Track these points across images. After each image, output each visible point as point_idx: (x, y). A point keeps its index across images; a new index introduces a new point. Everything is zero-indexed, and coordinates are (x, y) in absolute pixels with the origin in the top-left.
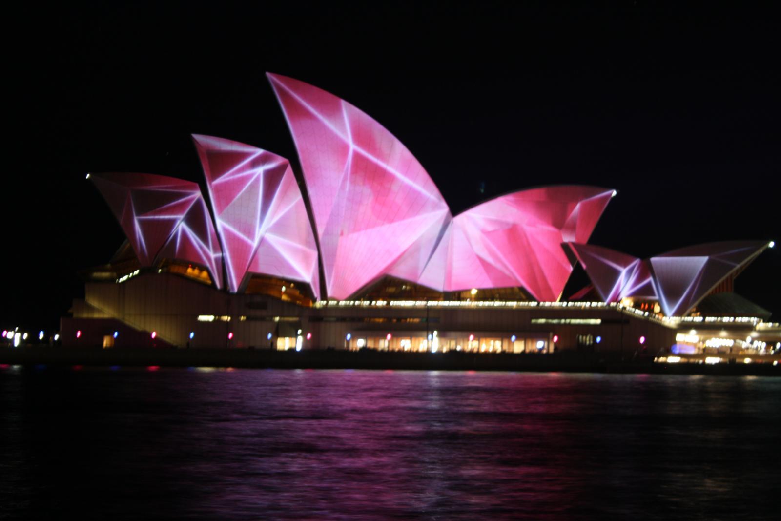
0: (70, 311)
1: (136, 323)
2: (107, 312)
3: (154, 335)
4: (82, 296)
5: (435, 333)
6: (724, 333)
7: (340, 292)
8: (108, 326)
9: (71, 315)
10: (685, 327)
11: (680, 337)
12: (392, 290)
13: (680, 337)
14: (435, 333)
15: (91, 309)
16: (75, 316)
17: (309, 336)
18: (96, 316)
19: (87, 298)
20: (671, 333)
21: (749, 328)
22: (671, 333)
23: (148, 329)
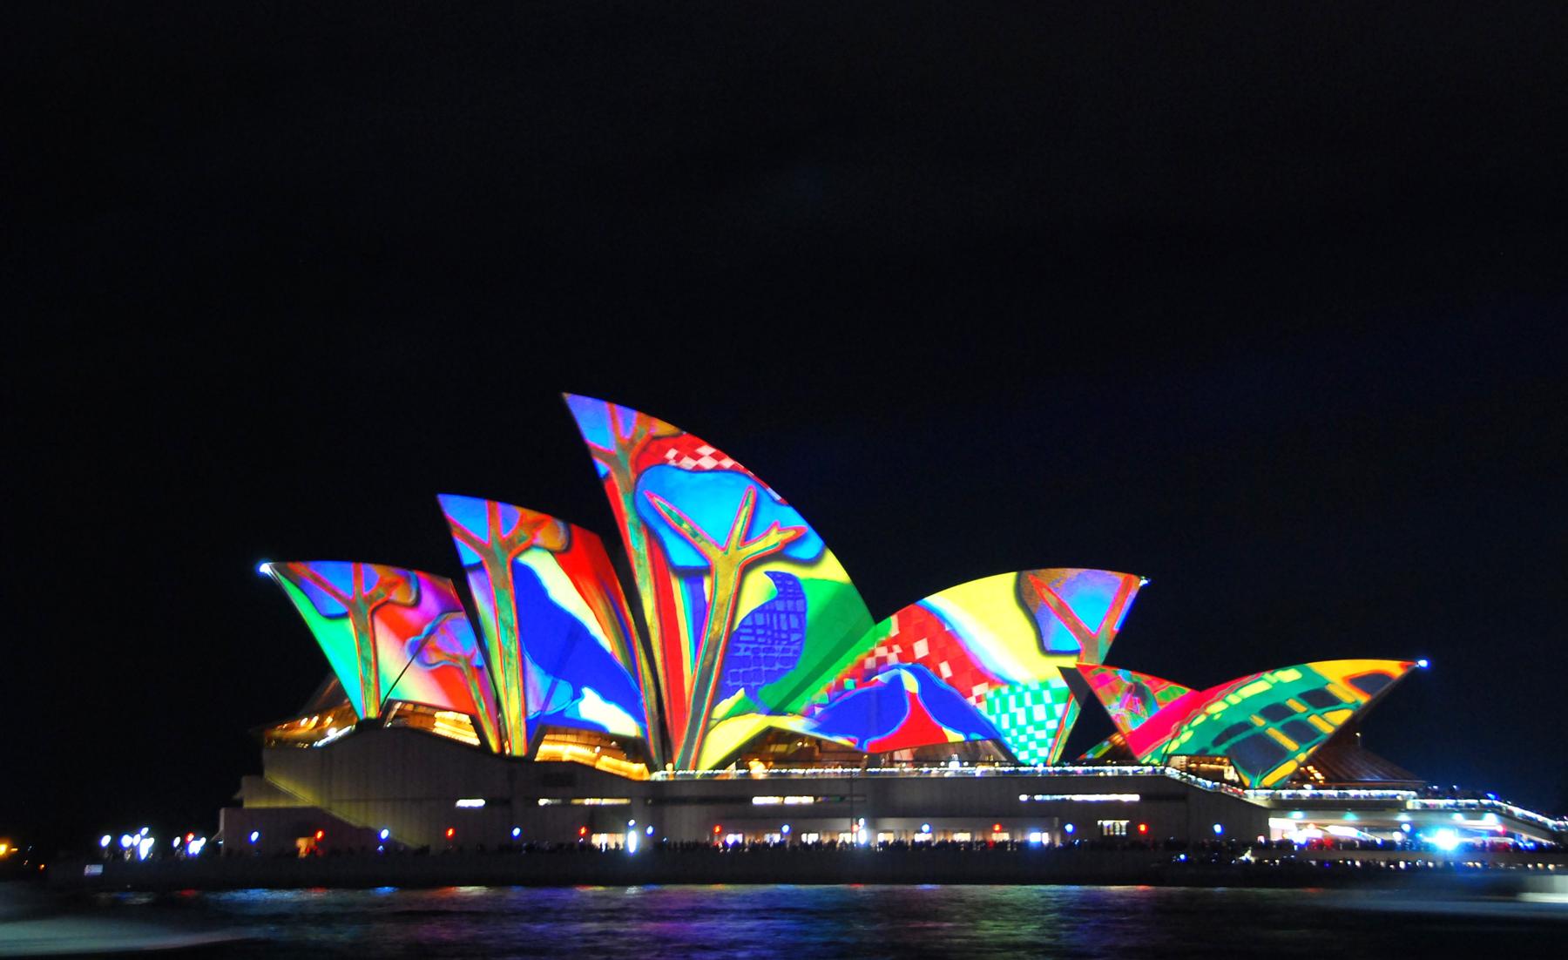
0: (237, 796)
1: (351, 814)
2: (304, 797)
3: (385, 834)
4: (257, 770)
5: (862, 821)
6: (1351, 817)
8: (304, 821)
9: (240, 803)
12: (781, 748)
14: (862, 821)
15: (274, 792)
16: (246, 805)
17: (650, 830)
18: (282, 804)
19: (266, 773)
20: (1259, 816)
21: (1399, 806)
22: (1259, 816)
23: (372, 825)
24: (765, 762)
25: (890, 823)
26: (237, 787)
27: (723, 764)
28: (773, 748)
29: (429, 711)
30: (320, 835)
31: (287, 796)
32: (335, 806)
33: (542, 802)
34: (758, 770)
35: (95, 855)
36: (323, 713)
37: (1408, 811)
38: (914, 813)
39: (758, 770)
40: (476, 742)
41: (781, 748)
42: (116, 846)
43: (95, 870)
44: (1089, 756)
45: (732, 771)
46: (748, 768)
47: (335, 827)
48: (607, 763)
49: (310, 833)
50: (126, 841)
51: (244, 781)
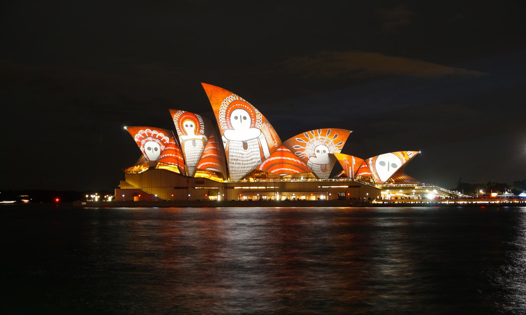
2: (135, 186)
4: (124, 179)
6: (401, 191)
8: (136, 192)
10: (385, 189)
12: (257, 174)
15: (128, 185)
18: (130, 188)
24: (253, 178)
25: (285, 193)
26: (119, 184)
27: (243, 179)
32: (144, 188)
34: (252, 180)
35: (85, 199)
39: (252, 180)
41: (257, 174)
42: (90, 198)
43: (85, 203)
47: (144, 194)
48: (213, 178)
49: (137, 195)
50: (92, 196)
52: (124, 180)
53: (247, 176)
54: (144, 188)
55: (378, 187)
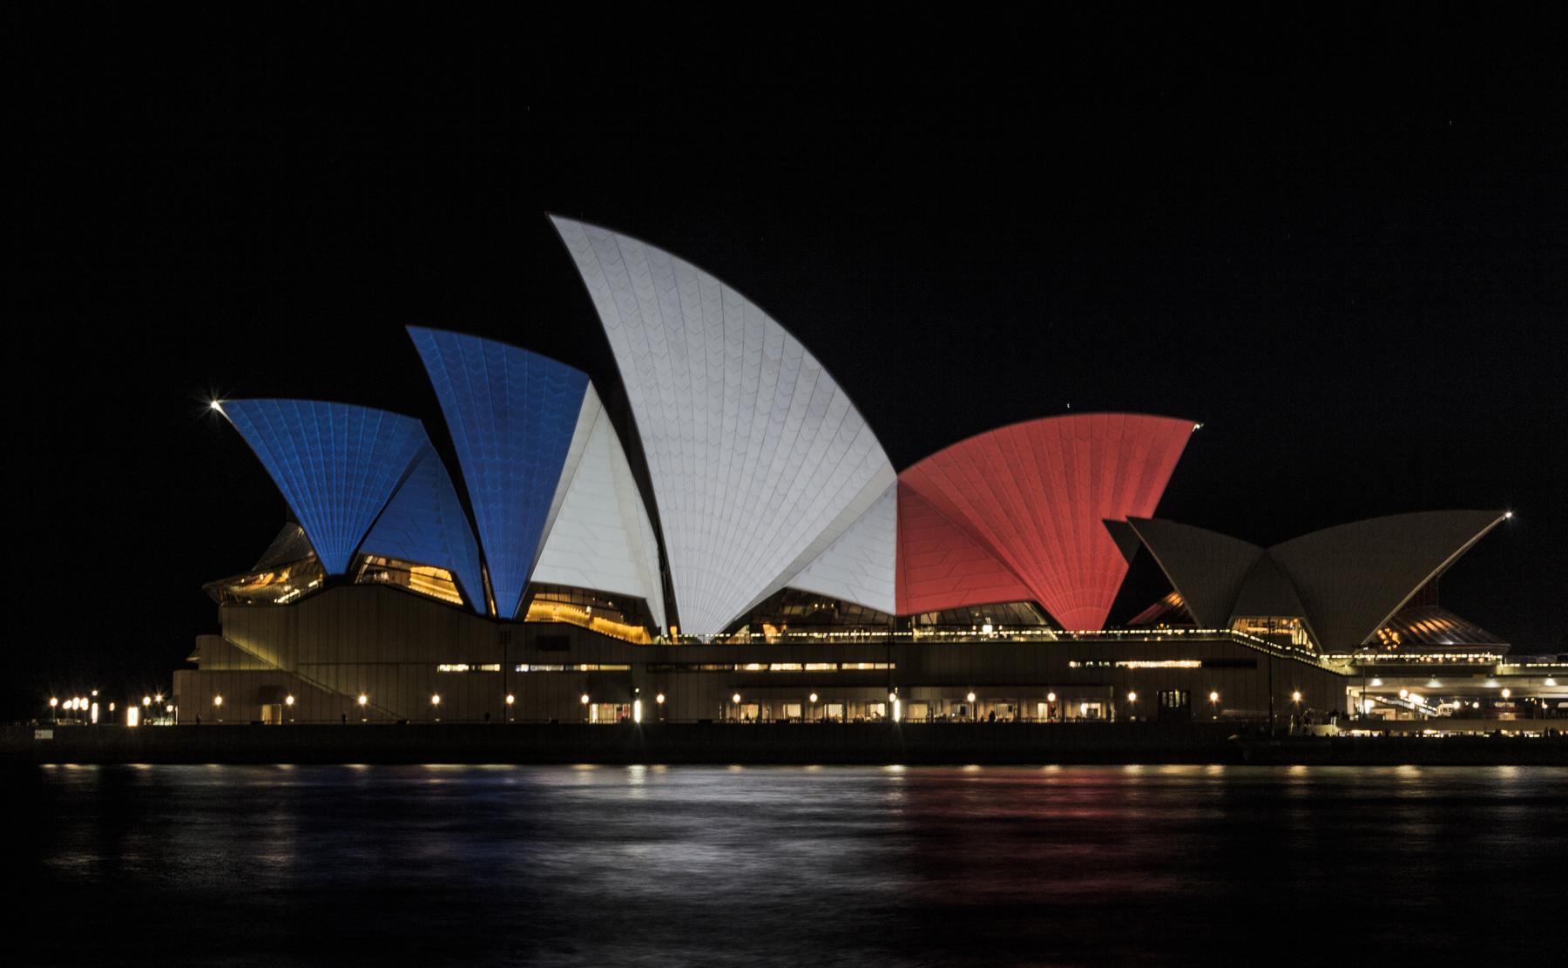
7: (704, 618)
10: (1363, 674)
11: (1353, 691)
12: (797, 610)
13: (1353, 691)
15: (237, 654)
16: (203, 668)
18: (244, 667)
19: (225, 633)
21: (1488, 671)
24: (778, 627)
25: (925, 693)
27: (733, 628)
28: (787, 610)
29: (405, 566)
30: (290, 700)
31: (252, 658)
32: (302, 670)
33: (497, 667)
34: (771, 633)
35: (46, 717)
36: (277, 569)
37: (1496, 676)
38: (953, 685)
39: (771, 633)
40: (459, 601)
41: (797, 610)
43: (47, 734)
44: (1052, 635)
45: (743, 634)
46: (762, 631)
48: (600, 624)
51: (202, 640)
52: (218, 631)
53: (754, 618)
54: (302, 670)
55: (1338, 664)
